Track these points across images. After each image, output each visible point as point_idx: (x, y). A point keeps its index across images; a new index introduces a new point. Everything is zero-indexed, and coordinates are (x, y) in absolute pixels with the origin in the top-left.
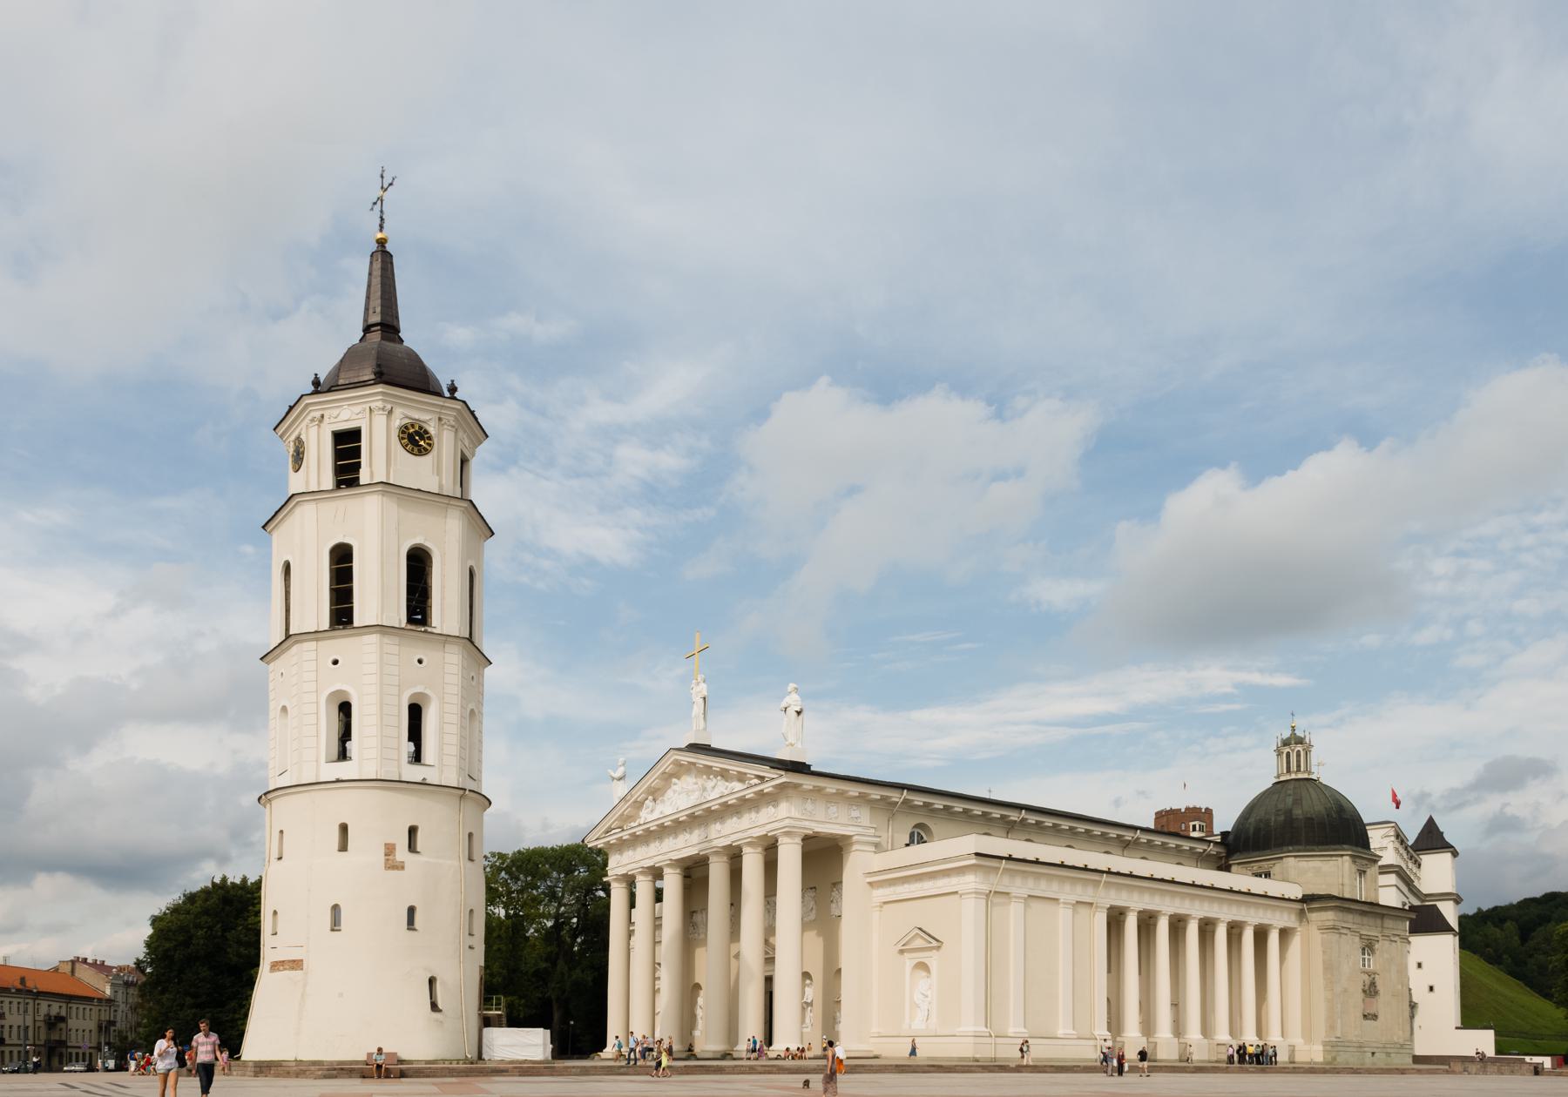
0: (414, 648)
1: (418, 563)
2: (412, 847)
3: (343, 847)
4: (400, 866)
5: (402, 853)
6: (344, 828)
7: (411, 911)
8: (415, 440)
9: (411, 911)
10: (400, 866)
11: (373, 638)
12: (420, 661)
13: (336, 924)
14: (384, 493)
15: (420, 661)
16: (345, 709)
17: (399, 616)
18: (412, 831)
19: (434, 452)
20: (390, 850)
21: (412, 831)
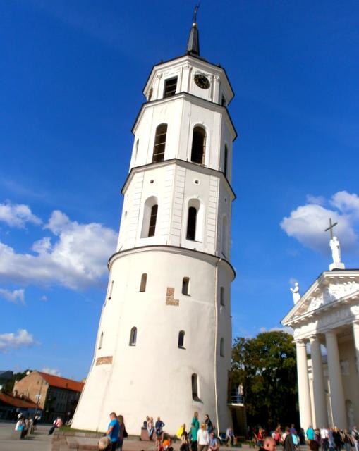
0: (195, 175)
1: (199, 135)
2: (185, 292)
3: (143, 289)
4: (176, 303)
5: (178, 294)
6: (144, 277)
7: (181, 335)
8: (202, 82)
9: (181, 335)
10: (176, 303)
11: (173, 167)
12: (197, 182)
13: (133, 340)
14: (185, 98)
15: (197, 182)
16: (155, 209)
17: (187, 156)
18: (186, 282)
19: (210, 88)
20: (170, 292)
21: (186, 282)
